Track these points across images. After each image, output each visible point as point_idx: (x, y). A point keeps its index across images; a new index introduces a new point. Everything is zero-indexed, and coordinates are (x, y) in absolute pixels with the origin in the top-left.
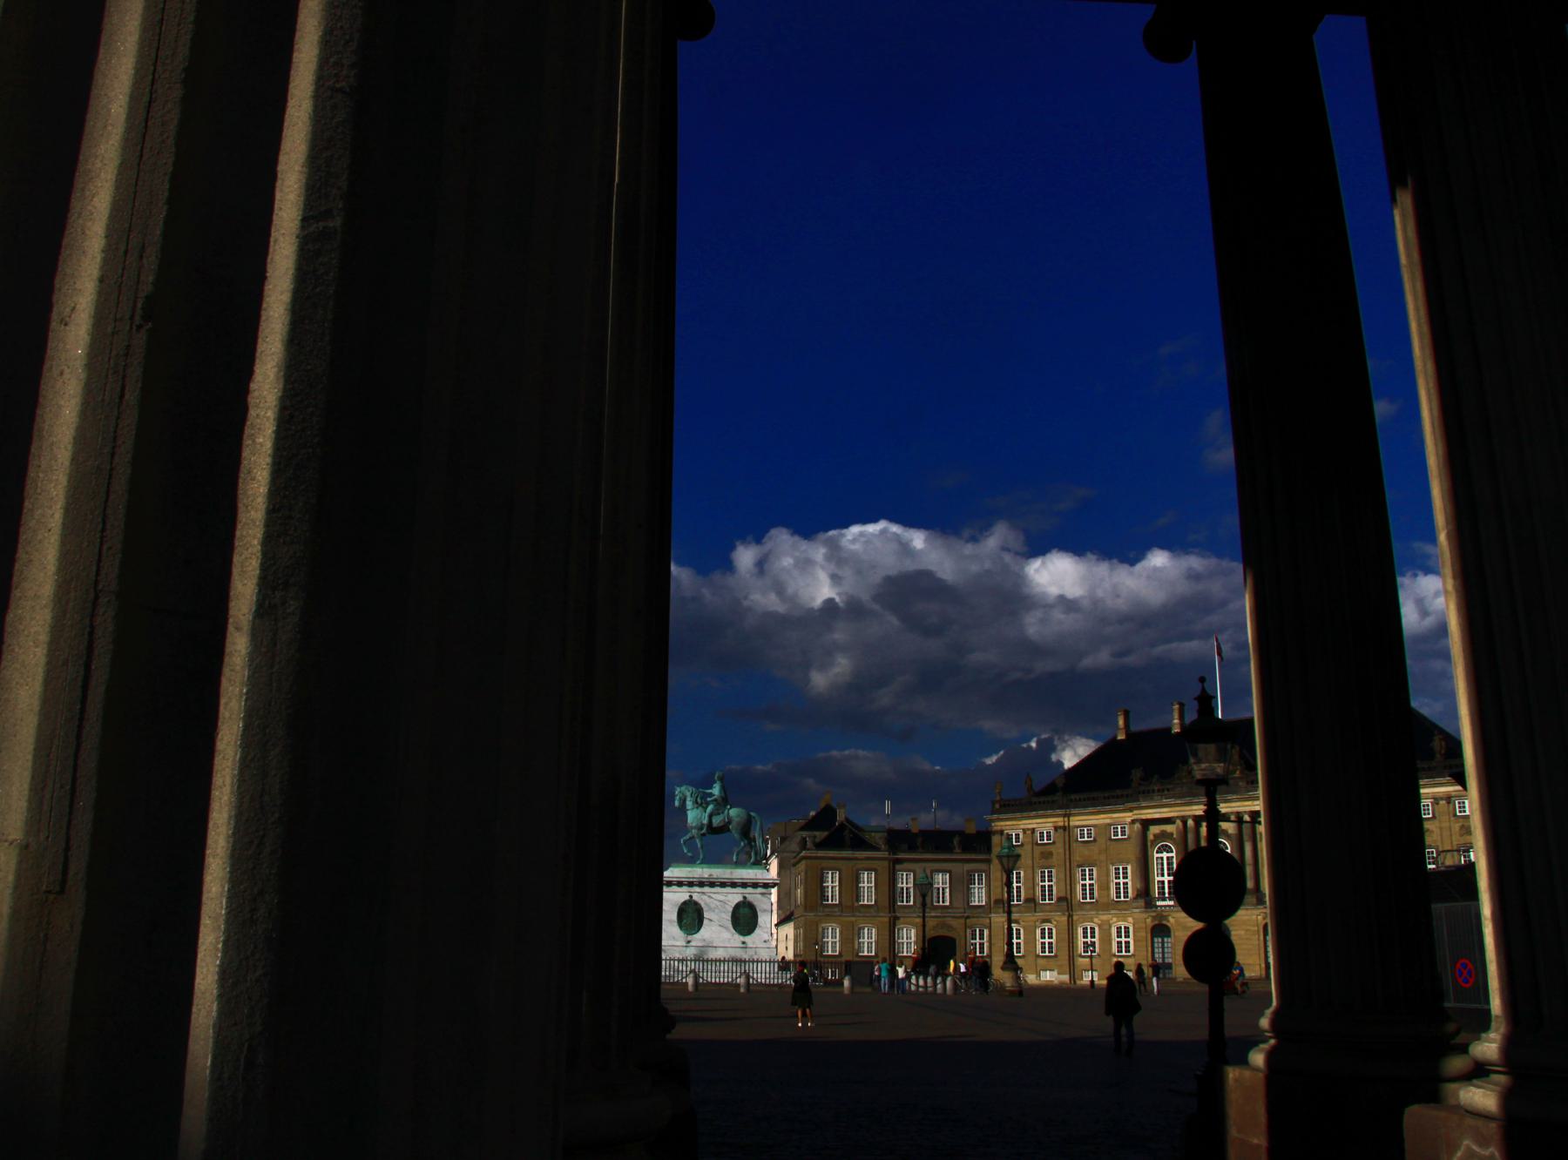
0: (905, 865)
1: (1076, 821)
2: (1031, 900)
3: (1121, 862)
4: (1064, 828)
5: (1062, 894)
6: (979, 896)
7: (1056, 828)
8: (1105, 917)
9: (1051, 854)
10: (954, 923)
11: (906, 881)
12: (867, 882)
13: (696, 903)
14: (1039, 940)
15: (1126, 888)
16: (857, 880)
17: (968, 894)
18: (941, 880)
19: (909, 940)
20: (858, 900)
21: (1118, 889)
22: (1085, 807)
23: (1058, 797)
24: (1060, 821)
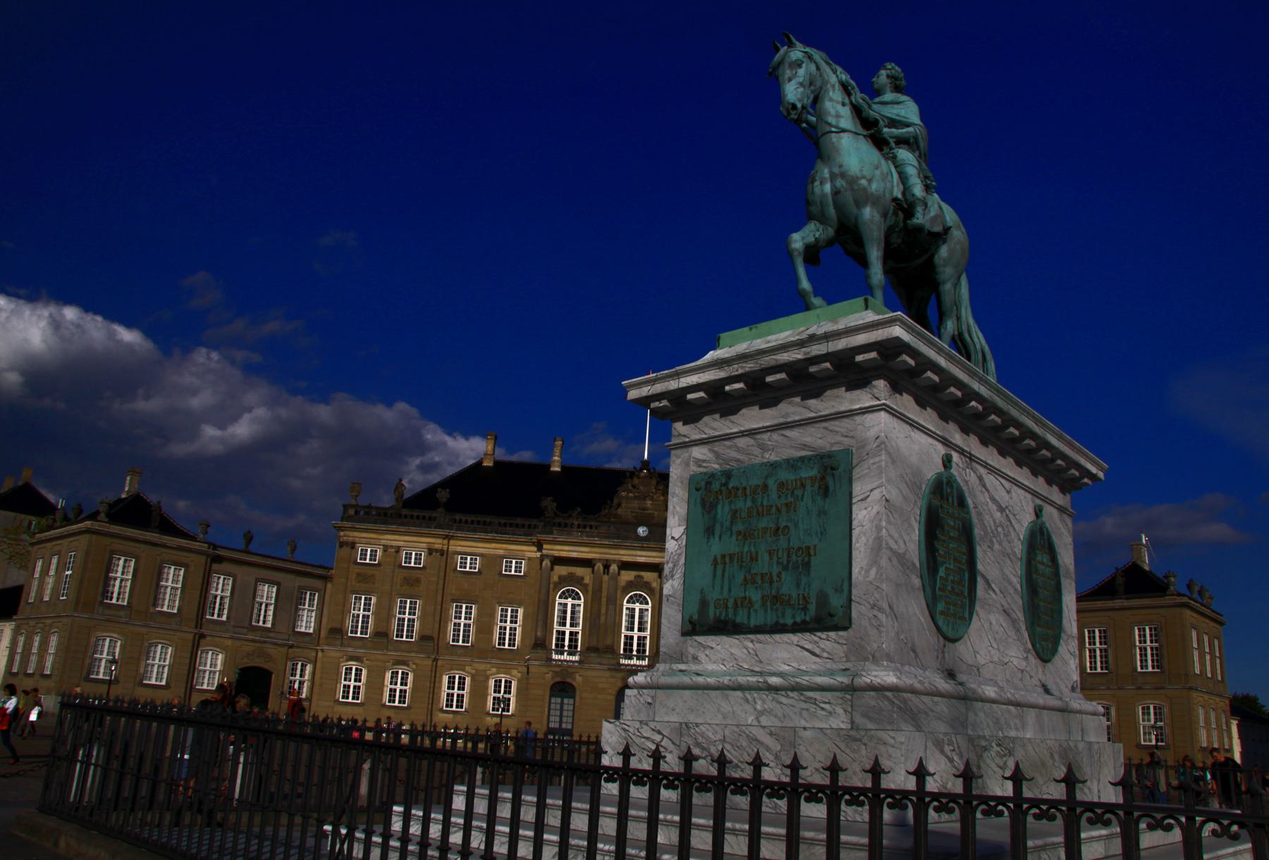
0: (225, 566)
1: (456, 546)
2: (382, 635)
3: (510, 603)
4: (442, 552)
5: (428, 633)
6: (307, 623)
7: (431, 551)
8: (482, 667)
9: (418, 581)
10: (270, 649)
11: (221, 587)
12: (173, 579)
14: (388, 686)
15: (513, 635)
16: (159, 576)
17: (295, 617)
18: (267, 593)
19: (213, 669)
20: (155, 605)
21: (457, 630)
22: (475, 531)
23: (439, 513)
24: (438, 543)
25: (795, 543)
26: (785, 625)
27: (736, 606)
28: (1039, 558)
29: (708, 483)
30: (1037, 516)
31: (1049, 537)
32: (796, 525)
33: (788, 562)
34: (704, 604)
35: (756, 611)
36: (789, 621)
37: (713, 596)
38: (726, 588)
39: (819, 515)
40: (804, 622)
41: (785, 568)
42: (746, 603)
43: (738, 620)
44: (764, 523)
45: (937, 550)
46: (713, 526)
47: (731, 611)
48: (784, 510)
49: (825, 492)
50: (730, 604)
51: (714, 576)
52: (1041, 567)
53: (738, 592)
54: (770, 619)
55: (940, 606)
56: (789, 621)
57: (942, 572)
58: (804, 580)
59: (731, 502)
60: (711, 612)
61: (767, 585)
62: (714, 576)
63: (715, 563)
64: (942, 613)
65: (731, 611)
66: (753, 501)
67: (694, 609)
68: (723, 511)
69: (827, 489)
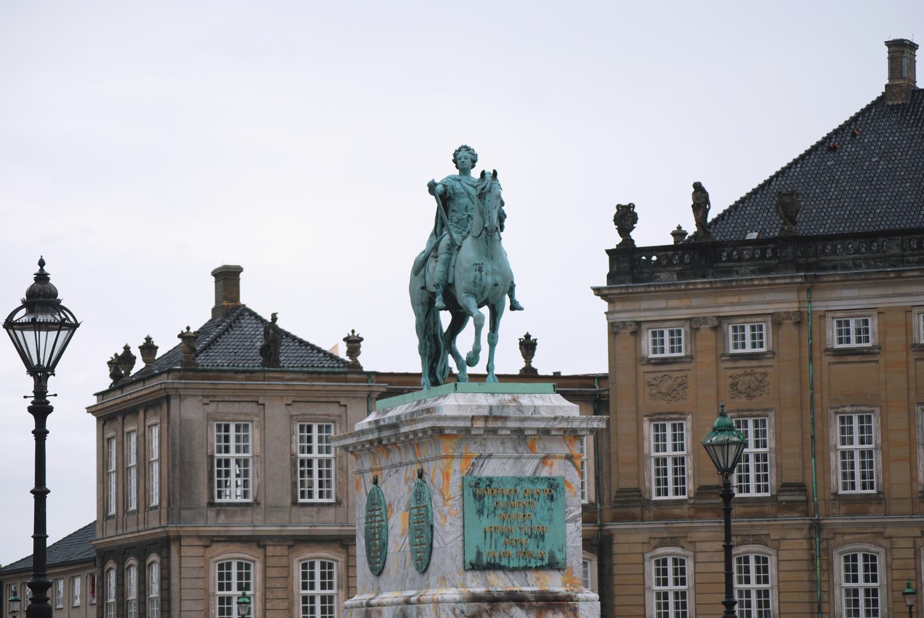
25: (535, 525)
27: (500, 556)
29: (477, 484)
34: (479, 554)
36: (534, 566)
37: (485, 550)
40: (542, 566)
41: (530, 537)
43: (502, 564)
44: (515, 511)
46: (483, 509)
48: (527, 505)
49: (552, 498)
50: (497, 555)
53: (501, 549)
54: (522, 563)
56: (534, 566)
58: (541, 544)
66: (508, 497)
68: (488, 501)
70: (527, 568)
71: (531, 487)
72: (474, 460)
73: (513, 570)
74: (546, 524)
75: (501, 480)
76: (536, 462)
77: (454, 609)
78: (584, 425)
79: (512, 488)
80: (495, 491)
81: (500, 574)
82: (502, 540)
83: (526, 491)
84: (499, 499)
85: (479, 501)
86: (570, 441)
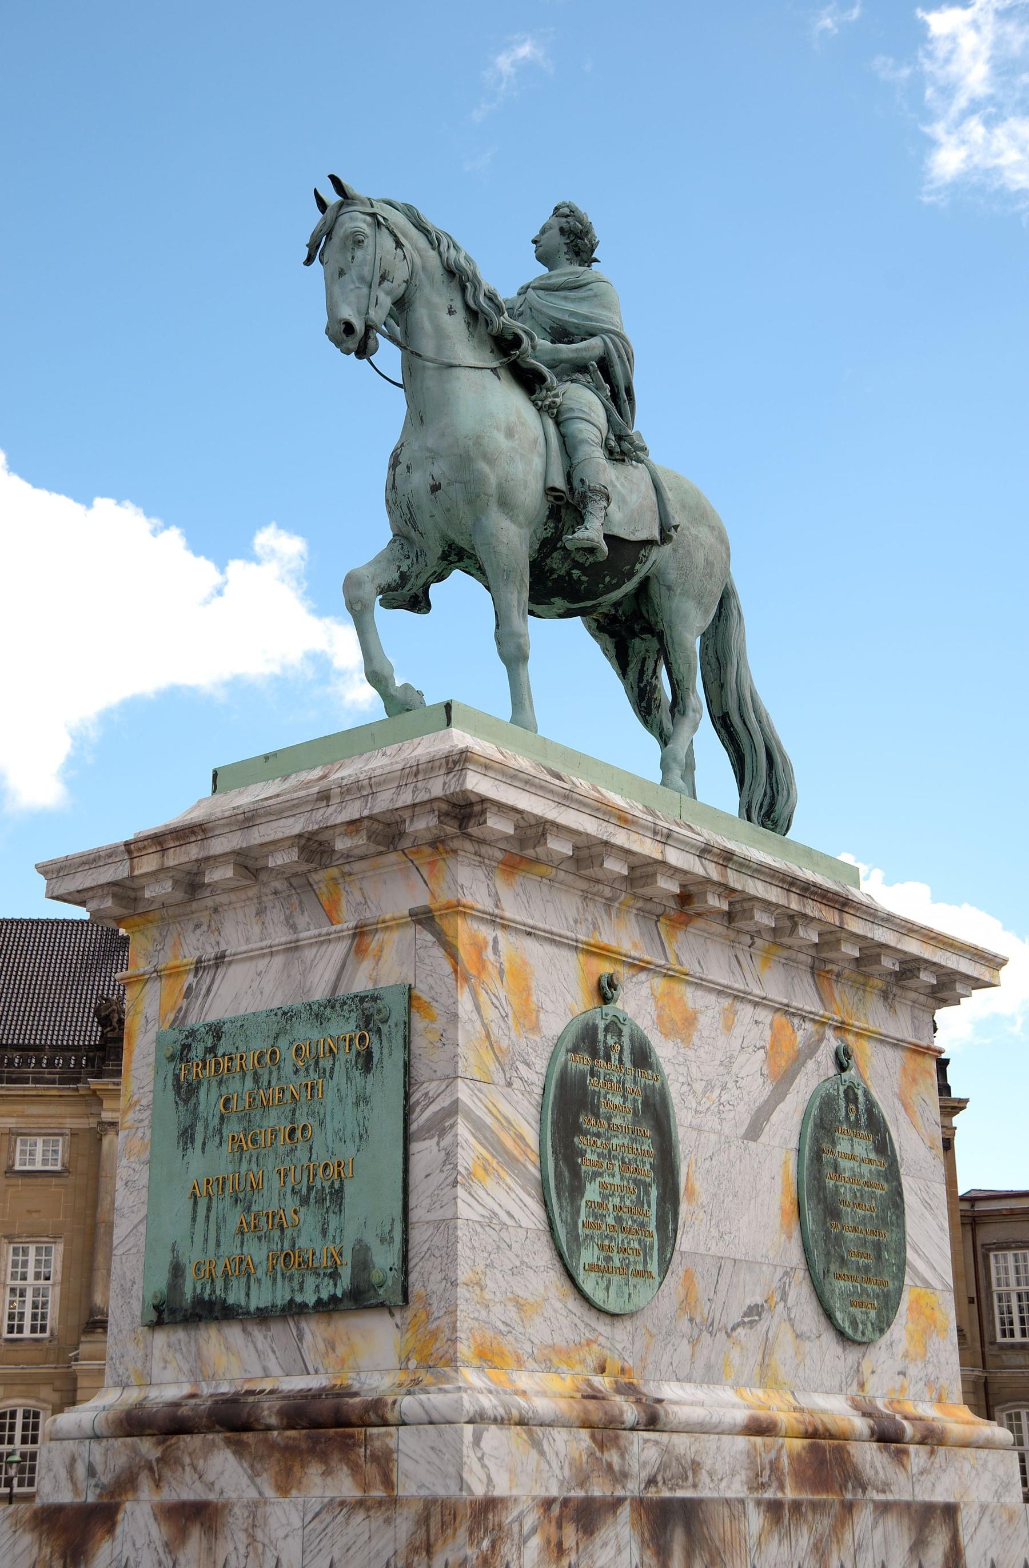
13: (643, 1057)
25: (321, 1156)
26: (304, 1305)
27: (226, 1276)
28: (843, 1146)
30: (842, 1068)
31: (871, 1105)
32: (321, 1123)
33: (310, 1189)
34: (177, 1270)
35: (259, 1281)
36: (311, 1299)
37: (191, 1256)
38: (212, 1242)
39: (357, 1104)
40: (333, 1298)
41: (305, 1201)
42: (244, 1269)
43: (231, 1300)
45: (582, 1154)
46: (193, 1126)
47: (219, 1284)
49: (366, 1061)
51: (194, 1219)
52: (845, 1164)
53: (230, 1248)
54: (282, 1295)
55: (588, 1255)
56: (311, 1299)
57: (592, 1192)
58: (334, 1221)
59: (220, 1083)
60: (189, 1288)
61: (277, 1233)
62: (194, 1219)
63: (194, 1196)
64: (591, 1268)
65: (219, 1284)
67: (161, 1282)
68: (208, 1100)
69: (369, 1056)
70: (293, 1311)
71: (315, 1035)
72: (190, 979)
73: (263, 1316)
74: (347, 1152)
75: (242, 1024)
76: (338, 950)
77: (73, 1460)
78: (406, 798)
79: (265, 1046)
80: (225, 1063)
81: (234, 1333)
82: (235, 1217)
83: (298, 1049)
84: (234, 1086)
85: (186, 1101)
86: (432, 864)
